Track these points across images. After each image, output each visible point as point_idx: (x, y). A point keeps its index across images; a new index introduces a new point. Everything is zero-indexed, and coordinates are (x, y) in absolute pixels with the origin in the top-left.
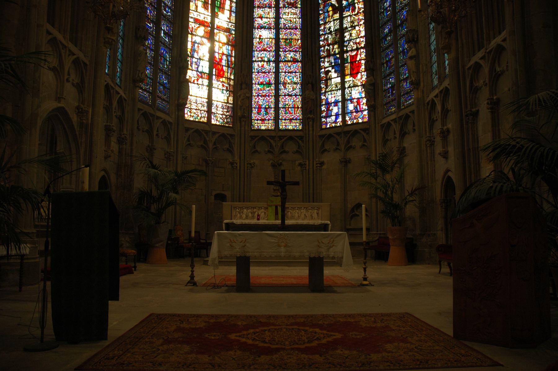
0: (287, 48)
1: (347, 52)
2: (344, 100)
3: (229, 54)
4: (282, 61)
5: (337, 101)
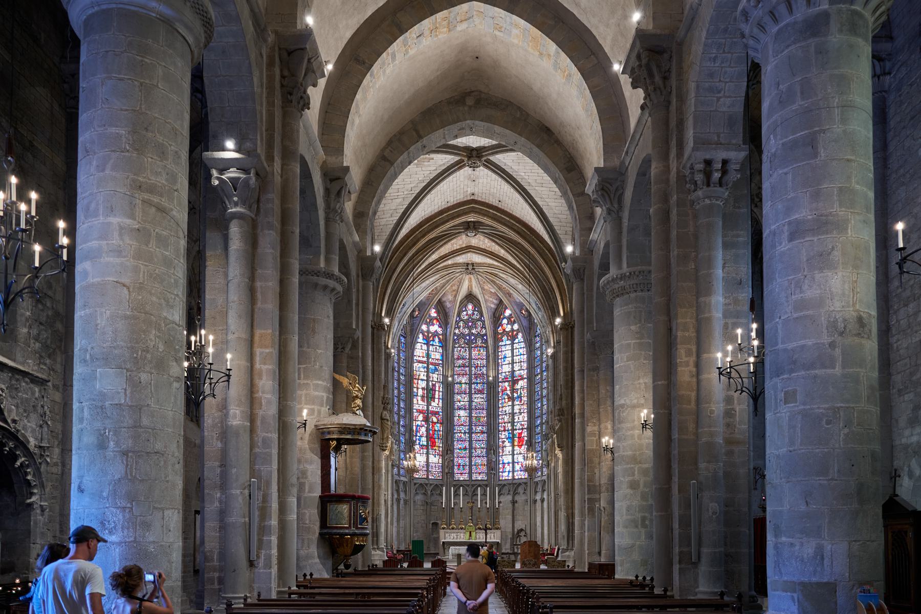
1: (516, 430)
2: (513, 462)
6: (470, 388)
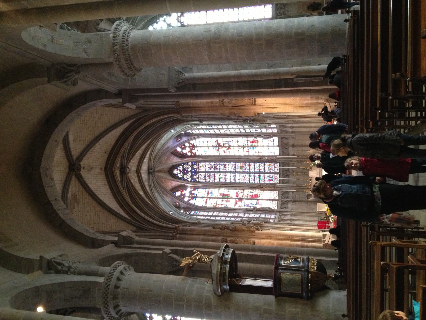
2: (268, 146)
6: (223, 172)
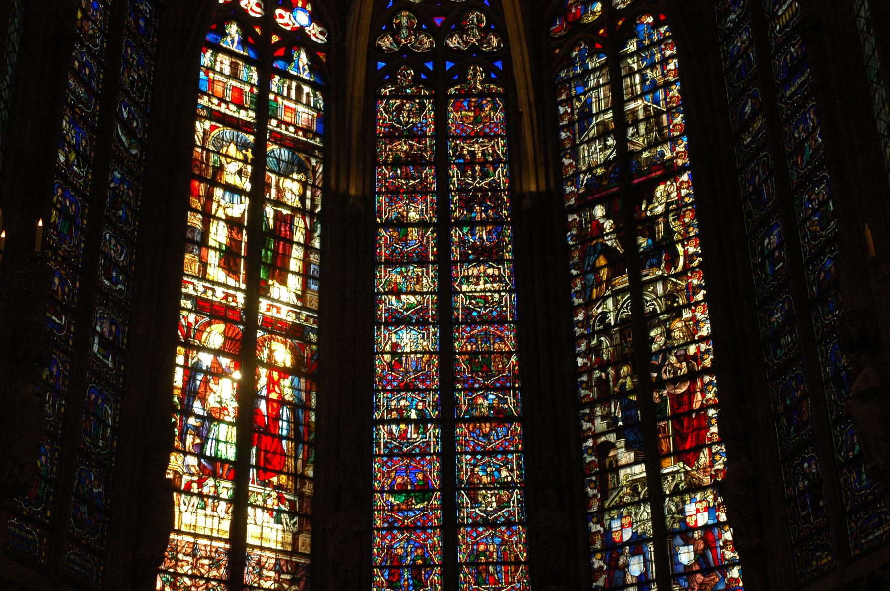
0: (476, 381)
1: (661, 384)
3: (300, 400)
4: (464, 421)
5: (639, 537)
6: (444, 242)
